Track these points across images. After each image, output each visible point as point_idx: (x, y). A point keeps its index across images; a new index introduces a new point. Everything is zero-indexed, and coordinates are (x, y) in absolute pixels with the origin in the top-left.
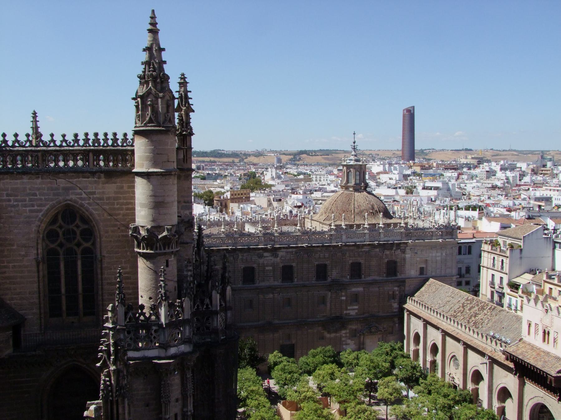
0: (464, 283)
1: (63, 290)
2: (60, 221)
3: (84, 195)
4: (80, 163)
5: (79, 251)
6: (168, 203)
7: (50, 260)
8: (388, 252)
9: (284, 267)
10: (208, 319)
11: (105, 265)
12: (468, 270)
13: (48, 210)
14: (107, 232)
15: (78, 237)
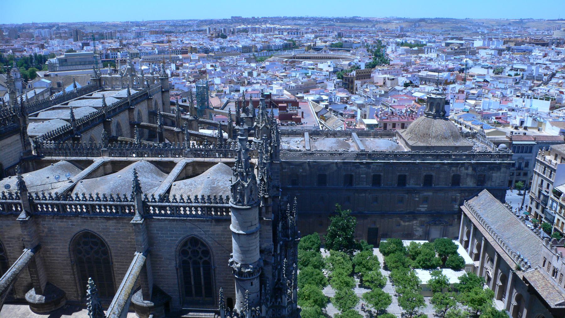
0: (522, 174)
1: (193, 283)
2: (189, 245)
3: (202, 232)
4: (199, 213)
5: (201, 262)
6: (252, 250)
7: (184, 266)
8: (454, 169)
9: (374, 176)
10: (279, 310)
11: (217, 272)
12: (527, 165)
13: (182, 240)
14: (217, 253)
15: (200, 255)
